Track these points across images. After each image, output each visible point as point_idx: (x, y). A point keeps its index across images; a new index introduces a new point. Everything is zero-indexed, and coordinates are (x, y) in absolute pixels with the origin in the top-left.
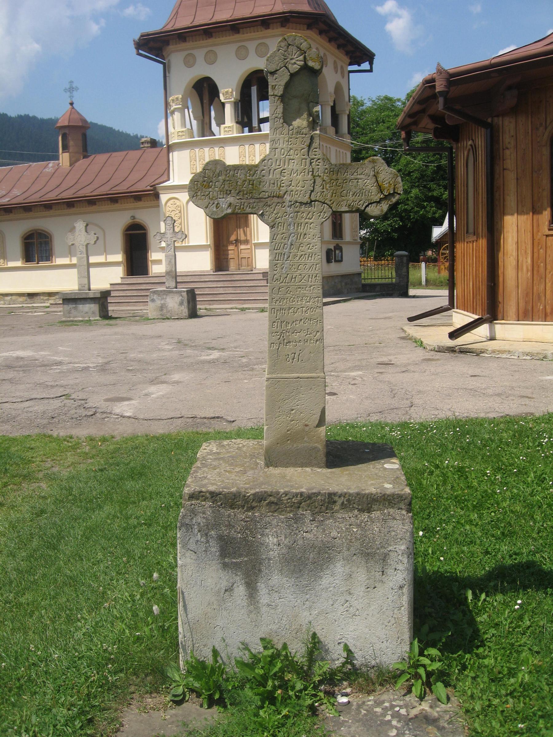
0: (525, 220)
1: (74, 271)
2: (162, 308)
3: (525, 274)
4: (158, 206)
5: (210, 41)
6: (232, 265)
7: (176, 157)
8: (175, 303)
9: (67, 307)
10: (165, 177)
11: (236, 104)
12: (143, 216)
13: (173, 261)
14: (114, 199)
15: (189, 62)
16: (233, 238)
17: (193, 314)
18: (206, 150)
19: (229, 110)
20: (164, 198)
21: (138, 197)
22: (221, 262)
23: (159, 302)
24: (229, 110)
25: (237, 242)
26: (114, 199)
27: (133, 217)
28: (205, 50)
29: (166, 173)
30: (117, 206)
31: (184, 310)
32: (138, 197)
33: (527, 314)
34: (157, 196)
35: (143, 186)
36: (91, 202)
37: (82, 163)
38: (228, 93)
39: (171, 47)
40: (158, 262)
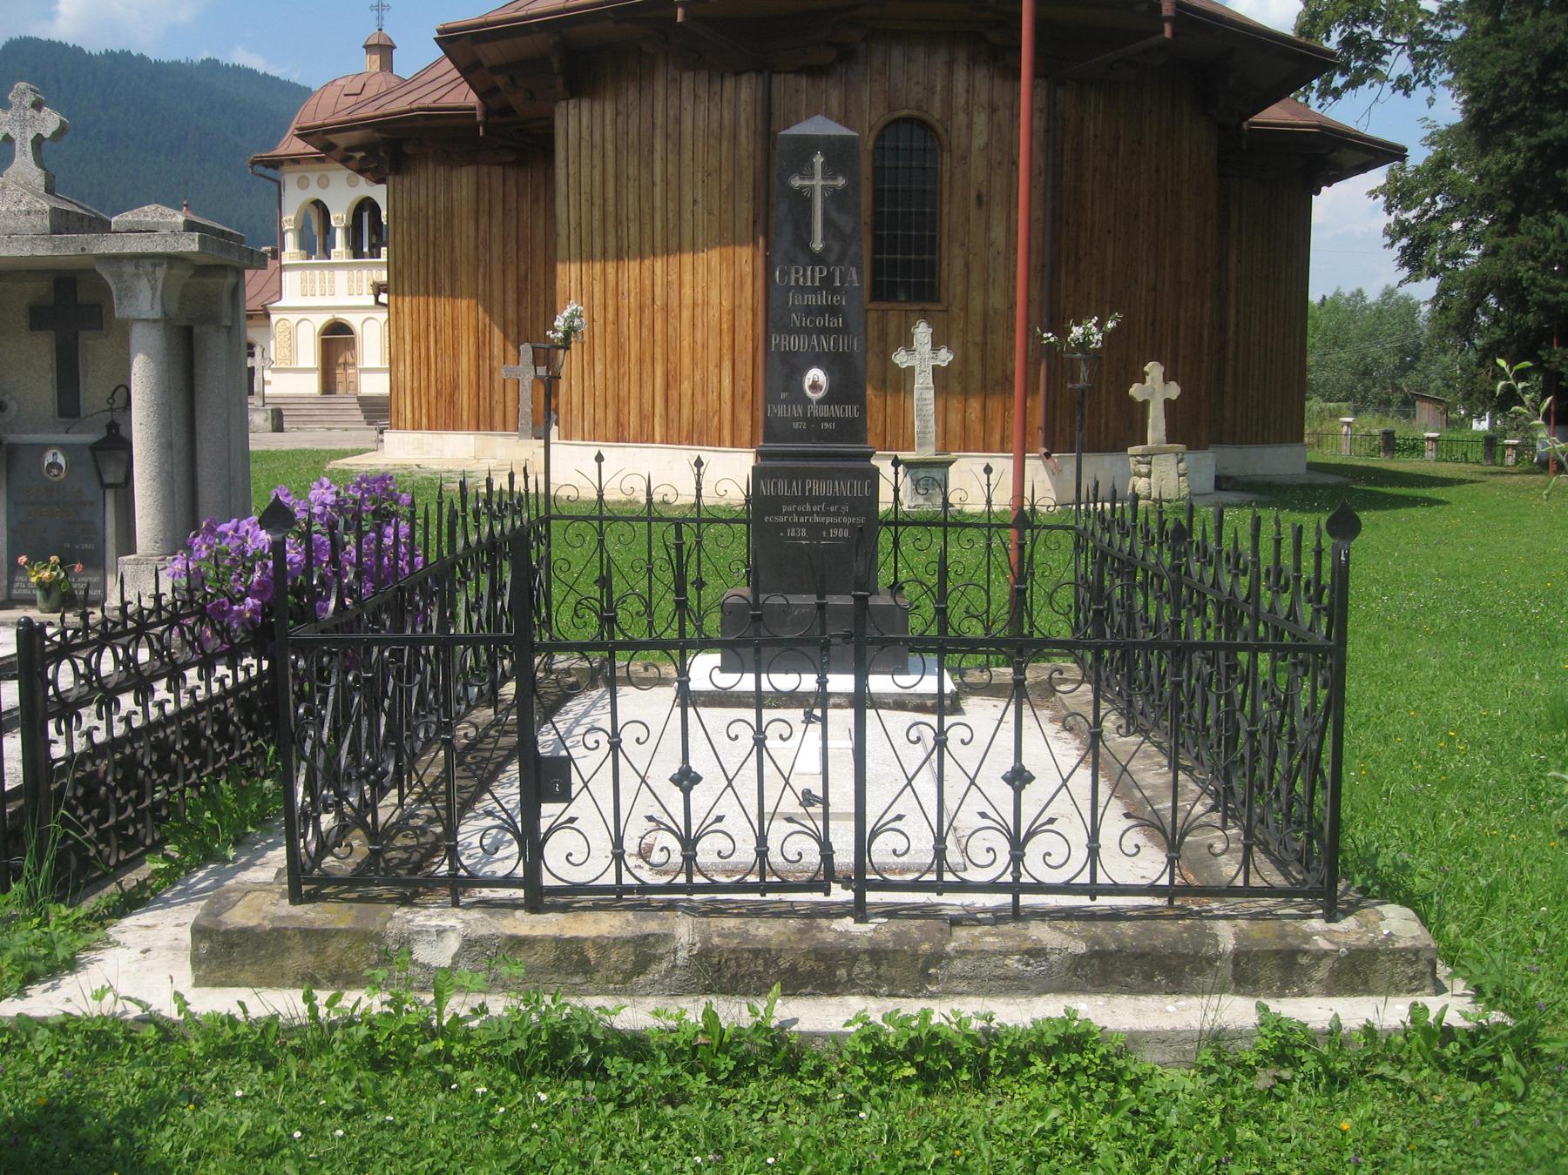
5: (323, 166)
6: (340, 389)
7: (286, 276)
11: (346, 229)
15: (303, 184)
16: (341, 360)
19: (340, 236)
20: (274, 318)
22: (328, 386)
24: (340, 236)
25: (345, 364)
28: (318, 174)
29: (279, 294)
31: (269, 425)
34: (268, 316)
38: (340, 218)
39: (285, 168)
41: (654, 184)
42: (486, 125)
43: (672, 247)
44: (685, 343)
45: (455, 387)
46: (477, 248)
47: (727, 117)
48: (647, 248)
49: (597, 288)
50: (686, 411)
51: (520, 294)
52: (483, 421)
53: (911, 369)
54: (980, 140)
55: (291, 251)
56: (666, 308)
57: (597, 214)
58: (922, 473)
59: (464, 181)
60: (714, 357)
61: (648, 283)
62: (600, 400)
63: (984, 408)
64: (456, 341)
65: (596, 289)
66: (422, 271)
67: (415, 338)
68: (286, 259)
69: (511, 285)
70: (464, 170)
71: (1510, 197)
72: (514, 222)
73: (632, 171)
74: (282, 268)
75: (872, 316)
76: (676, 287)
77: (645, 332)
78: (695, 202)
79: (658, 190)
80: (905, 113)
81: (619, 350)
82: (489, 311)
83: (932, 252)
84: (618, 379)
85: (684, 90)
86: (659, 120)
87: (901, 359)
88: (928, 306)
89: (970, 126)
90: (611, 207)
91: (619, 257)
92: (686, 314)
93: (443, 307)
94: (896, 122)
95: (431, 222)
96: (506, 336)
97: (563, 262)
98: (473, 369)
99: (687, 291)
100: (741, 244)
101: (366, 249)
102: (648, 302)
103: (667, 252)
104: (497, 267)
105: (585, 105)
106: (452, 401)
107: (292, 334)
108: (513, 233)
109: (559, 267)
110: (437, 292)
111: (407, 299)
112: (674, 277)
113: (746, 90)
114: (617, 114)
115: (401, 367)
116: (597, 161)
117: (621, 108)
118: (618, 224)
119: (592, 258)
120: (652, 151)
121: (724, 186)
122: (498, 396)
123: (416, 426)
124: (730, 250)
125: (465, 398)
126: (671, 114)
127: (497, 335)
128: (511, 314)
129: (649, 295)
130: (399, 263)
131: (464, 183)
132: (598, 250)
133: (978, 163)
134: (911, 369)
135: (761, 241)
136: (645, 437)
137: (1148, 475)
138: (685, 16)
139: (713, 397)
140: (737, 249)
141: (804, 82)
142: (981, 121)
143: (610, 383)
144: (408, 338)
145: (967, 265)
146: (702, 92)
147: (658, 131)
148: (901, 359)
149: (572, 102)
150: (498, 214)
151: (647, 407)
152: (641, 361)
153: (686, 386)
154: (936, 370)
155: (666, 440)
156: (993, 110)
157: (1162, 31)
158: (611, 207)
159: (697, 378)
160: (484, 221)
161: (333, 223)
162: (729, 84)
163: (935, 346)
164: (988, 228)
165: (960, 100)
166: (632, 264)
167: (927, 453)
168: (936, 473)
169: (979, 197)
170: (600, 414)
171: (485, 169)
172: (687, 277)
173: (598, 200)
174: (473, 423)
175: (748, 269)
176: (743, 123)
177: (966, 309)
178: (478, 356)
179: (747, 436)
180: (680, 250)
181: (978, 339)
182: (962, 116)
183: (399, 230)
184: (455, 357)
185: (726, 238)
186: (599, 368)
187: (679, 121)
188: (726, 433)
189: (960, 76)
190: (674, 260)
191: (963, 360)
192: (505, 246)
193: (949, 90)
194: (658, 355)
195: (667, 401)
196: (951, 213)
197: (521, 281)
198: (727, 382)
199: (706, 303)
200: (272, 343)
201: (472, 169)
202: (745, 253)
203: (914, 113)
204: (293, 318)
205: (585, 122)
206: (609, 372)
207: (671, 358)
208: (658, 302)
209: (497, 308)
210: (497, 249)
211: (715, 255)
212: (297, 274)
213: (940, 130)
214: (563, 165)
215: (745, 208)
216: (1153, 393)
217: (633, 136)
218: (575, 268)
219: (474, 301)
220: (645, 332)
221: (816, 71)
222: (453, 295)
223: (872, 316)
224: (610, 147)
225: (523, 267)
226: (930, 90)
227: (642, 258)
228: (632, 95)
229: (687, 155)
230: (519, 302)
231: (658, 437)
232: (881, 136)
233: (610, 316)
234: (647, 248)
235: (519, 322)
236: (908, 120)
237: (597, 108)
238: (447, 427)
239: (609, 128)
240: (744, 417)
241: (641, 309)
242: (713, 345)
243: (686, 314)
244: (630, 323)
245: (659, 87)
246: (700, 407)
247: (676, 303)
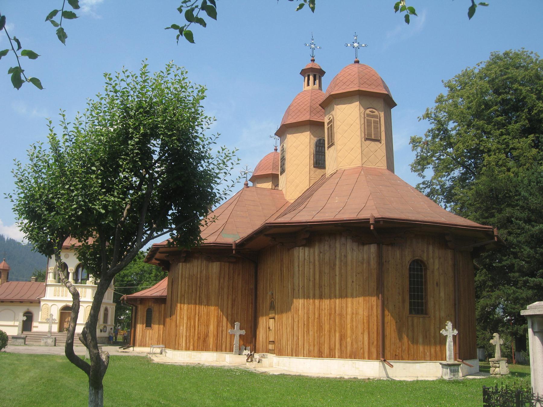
0: (141, 325)
1: (17, 328)
2: (46, 343)
3: (140, 337)
4: (39, 306)
5: (67, 251)
7: (48, 289)
8: (50, 341)
9: (13, 340)
10: (43, 294)
11: (74, 273)
12: (32, 309)
13: (50, 328)
14: (21, 302)
17: (55, 345)
18: (61, 288)
20: (42, 303)
21: (31, 302)
23: (45, 341)
24: (71, 276)
26: (21, 302)
27: (28, 309)
30: (22, 304)
31: (53, 344)
32: (31, 302)
33: (140, 346)
34: (40, 302)
35: (33, 298)
36: (12, 302)
37: (6, 284)
40: (38, 327)
41: (336, 275)
42: (235, 250)
43: (343, 295)
44: (349, 326)
45: (207, 336)
46: (219, 289)
47: (365, 256)
48: (332, 295)
49: (311, 307)
50: (349, 348)
51: (233, 306)
52: (218, 348)
53: (447, 336)
54: (436, 267)
55: (50, 278)
56: (341, 315)
57: (311, 283)
58: (452, 368)
59: (214, 267)
60: (360, 330)
61: (333, 306)
62: (312, 344)
63: (441, 348)
64: (208, 320)
65: (311, 307)
66: (193, 296)
67: (189, 318)
68: (49, 283)
69: (230, 302)
70: (215, 264)
71: (490, 281)
72: (232, 281)
73: (327, 271)
74: (46, 285)
75: (410, 319)
76: (345, 308)
77: (331, 322)
78: (353, 282)
79: (337, 278)
80: (417, 258)
81: (320, 328)
82: (222, 311)
83: (422, 299)
84: (319, 337)
85: (348, 248)
86: (338, 256)
87: (443, 332)
88: (425, 316)
89: (434, 262)
90: (317, 281)
91: (321, 297)
92: (349, 317)
93: (203, 309)
94: (414, 261)
95: (199, 279)
96: (227, 320)
97: (296, 298)
98: (215, 330)
99: (349, 310)
100: (372, 296)
101: (80, 281)
102: (333, 312)
103: (341, 297)
104: (225, 296)
105: (307, 249)
106: (205, 341)
107: (48, 309)
108: (231, 284)
109: (295, 300)
110: (200, 303)
111: (197, 306)
112: (344, 305)
113: (373, 248)
114: (320, 252)
115: (181, 328)
116: (312, 267)
117: (322, 251)
118: (320, 287)
119: (308, 297)
120: (335, 265)
121: (365, 278)
122: (224, 340)
123: (187, 349)
124: (367, 298)
125: (211, 340)
126: (343, 254)
127: (225, 319)
128: (230, 312)
129: (333, 310)
130: (183, 292)
131: (215, 268)
132: (311, 295)
133: (436, 273)
134: (447, 336)
135: (380, 295)
136: (331, 355)
137: (499, 367)
138: (374, 227)
139: (360, 344)
140: (370, 298)
141: (390, 248)
142: (437, 261)
143: (316, 338)
144: (185, 318)
145: (435, 304)
146: (355, 248)
147: (337, 259)
148: (443, 332)
149: (301, 248)
150: (226, 279)
151: (332, 346)
152: (330, 332)
153: (349, 340)
154: (453, 335)
155: (341, 357)
156: (440, 258)
157: (494, 239)
158: (317, 281)
159: (354, 337)
160: (222, 281)
161: (69, 271)
162: (366, 248)
163: (453, 330)
164: (439, 293)
165: (431, 255)
166: (326, 300)
167: (450, 361)
168: (456, 368)
169: (437, 284)
170: (311, 348)
171: (223, 263)
172: (349, 305)
173: (312, 279)
174: (215, 349)
175: (375, 303)
176: (372, 259)
177: (435, 316)
178: (218, 326)
179: (375, 355)
180: (346, 297)
181: (438, 326)
182: (432, 259)
183: (183, 281)
184: (208, 326)
185: (365, 293)
186: (311, 333)
187: (346, 256)
188: (366, 355)
189: (431, 248)
190: (344, 300)
191: (459, 334)
192: (228, 289)
193: (428, 251)
194: (337, 329)
195: (341, 345)
196: (430, 286)
197: (234, 301)
198: (366, 338)
199: (357, 314)
200: (40, 313)
201: (218, 263)
202: (374, 299)
203: (419, 258)
204: (50, 304)
205: (306, 254)
206: (316, 335)
207: (343, 331)
208: (337, 312)
209: (225, 310)
210: (226, 290)
211: (361, 299)
212: (53, 288)
213: (426, 263)
214: (297, 267)
215: (373, 284)
216: (497, 343)
217: (327, 259)
218: (301, 301)
219: (217, 307)
220: (331, 322)
221: (392, 244)
222: (208, 304)
223: (410, 319)
224: (317, 263)
225: (234, 296)
226: (423, 251)
227: (330, 299)
228: (327, 247)
229: (349, 268)
230: (232, 308)
231: (337, 356)
232: (410, 265)
233: (316, 316)
234: (332, 295)
235: (232, 315)
236: (418, 260)
237: (312, 250)
238: (202, 350)
239: (317, 257)
240: (374, 350)
241: (330, 315)
242: (360, 327)
243: (349, 317)
244: (325, 319)
245: (338, 245)
246: (355, 346)
247: (345, 313)
